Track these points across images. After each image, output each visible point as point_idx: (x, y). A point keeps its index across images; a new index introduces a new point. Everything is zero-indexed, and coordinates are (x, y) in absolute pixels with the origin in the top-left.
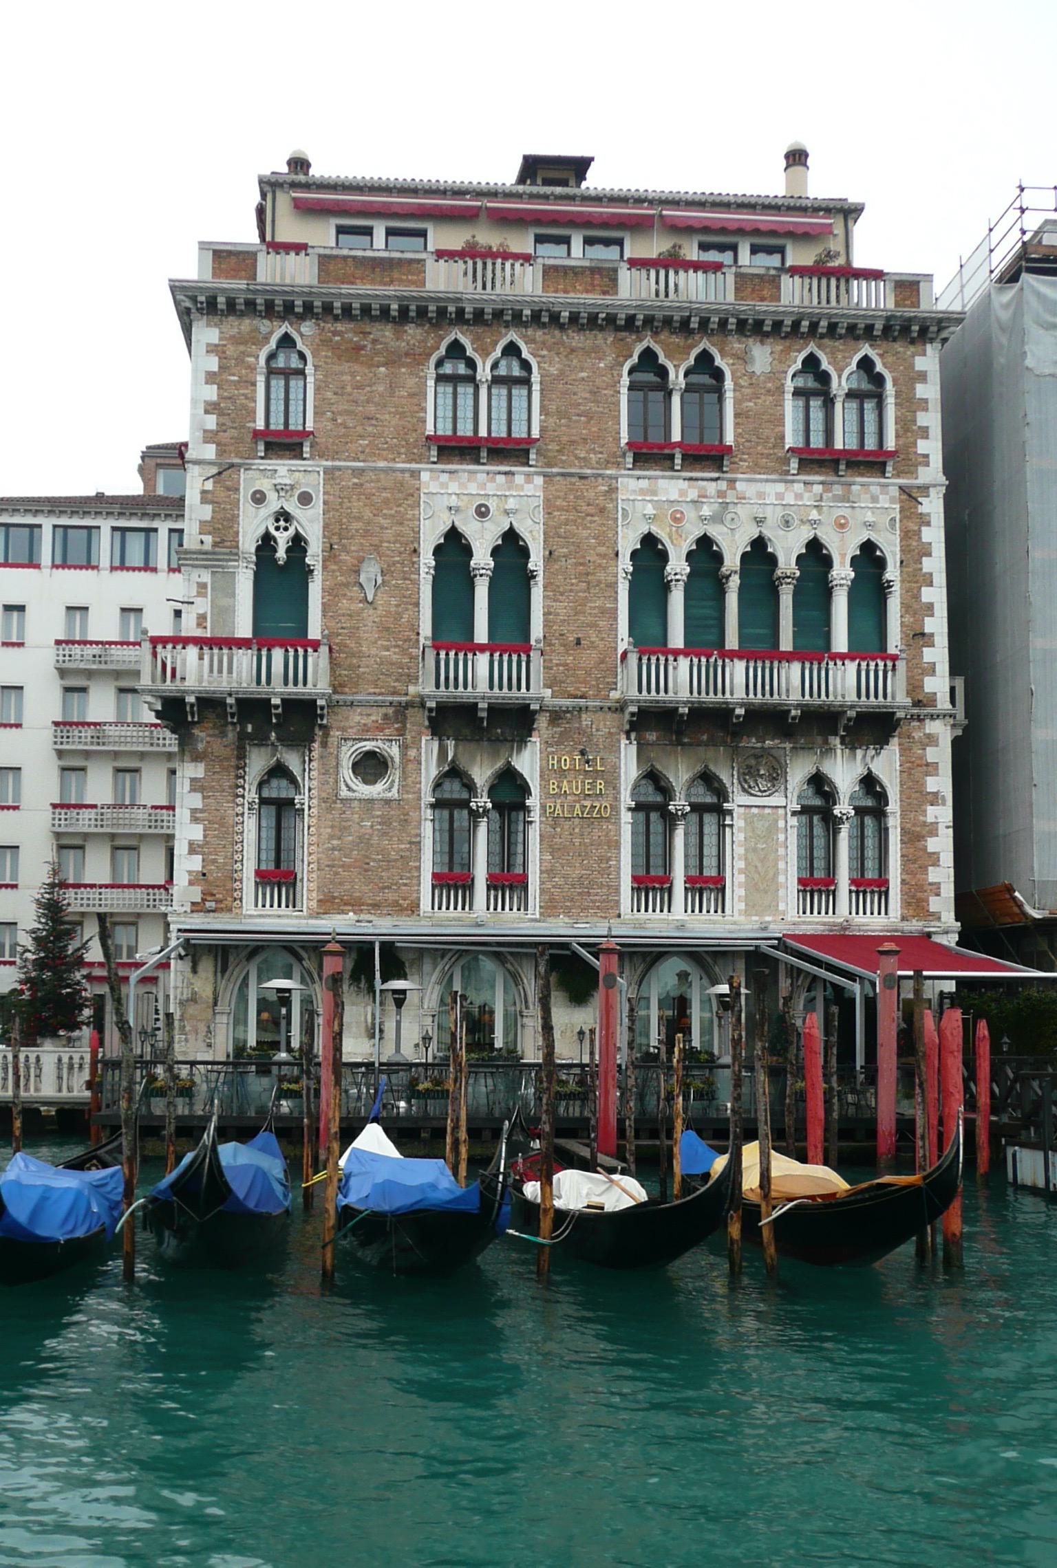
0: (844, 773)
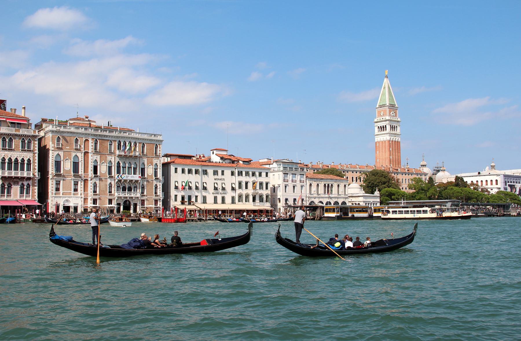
0: (25, 183)
